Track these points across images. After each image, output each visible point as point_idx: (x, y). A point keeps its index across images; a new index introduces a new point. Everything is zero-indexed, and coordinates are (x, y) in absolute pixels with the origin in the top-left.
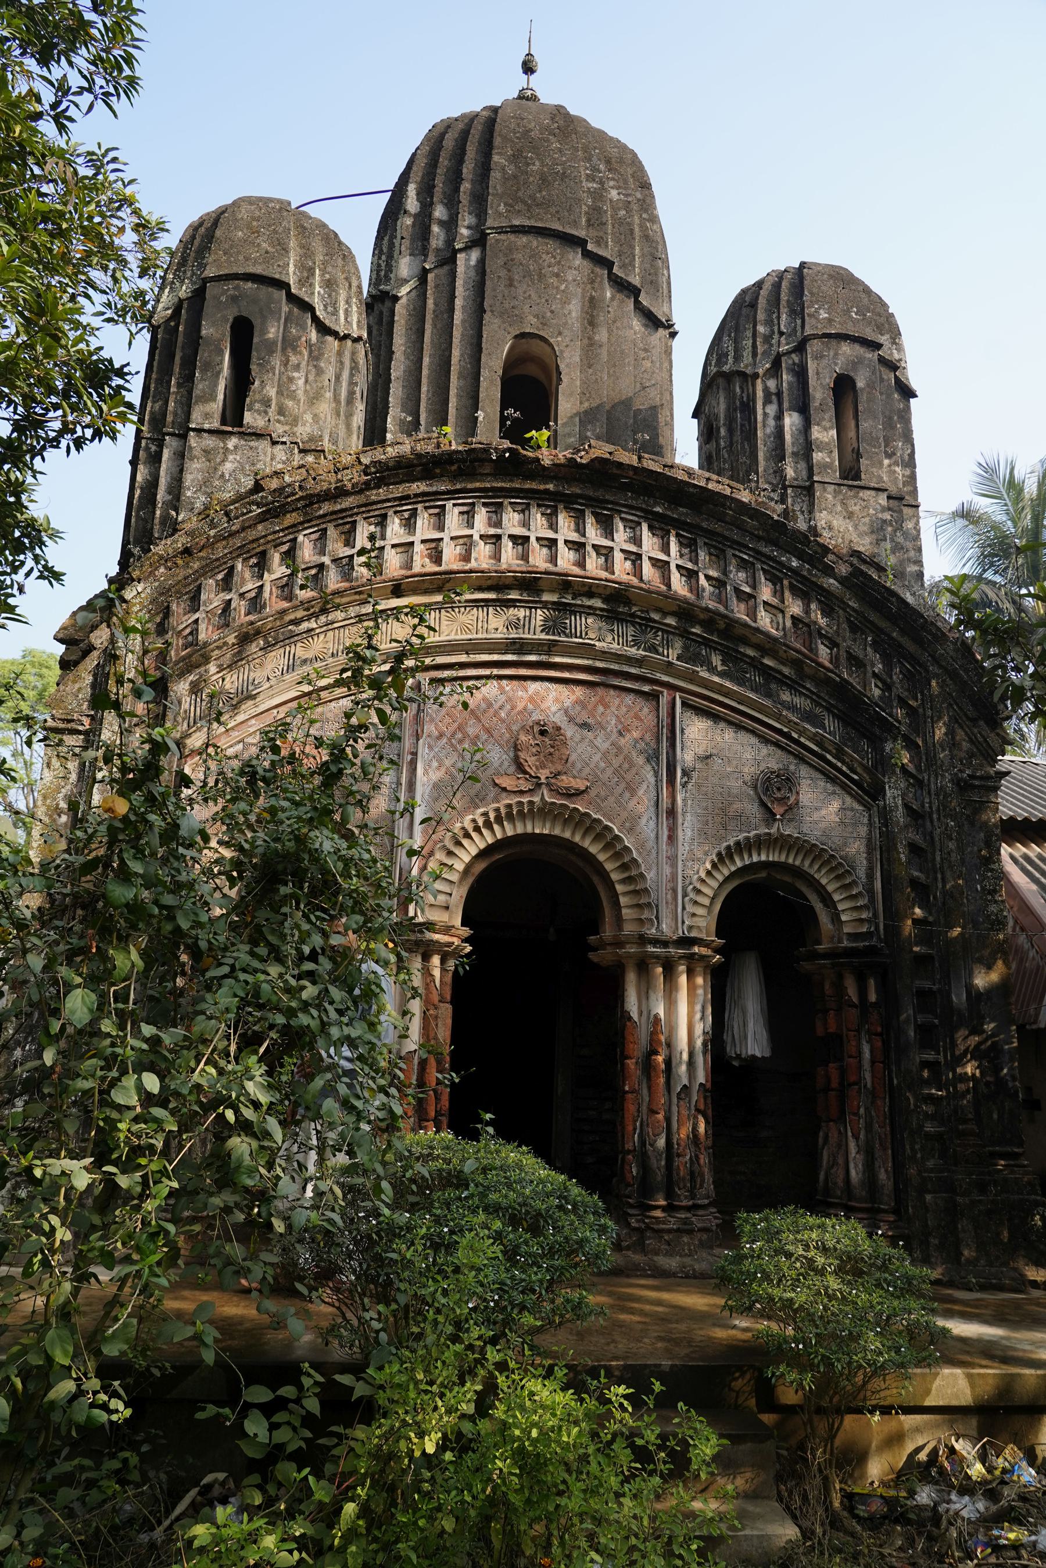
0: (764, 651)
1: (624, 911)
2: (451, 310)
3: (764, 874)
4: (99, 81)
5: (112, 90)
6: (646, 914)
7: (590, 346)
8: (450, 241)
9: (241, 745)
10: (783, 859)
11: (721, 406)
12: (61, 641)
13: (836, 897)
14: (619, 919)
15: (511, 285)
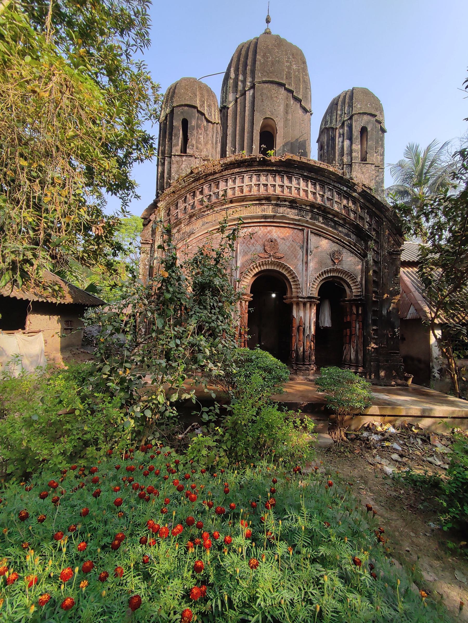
0: (334, 216)
2: (245, 111)
4: (139, 41)
5: (142, 45)
7: (286, 120)
8: (244, 87)
11: (325, 140)
12: (142, 218)
13: (351, 285)
15: (263, 101)
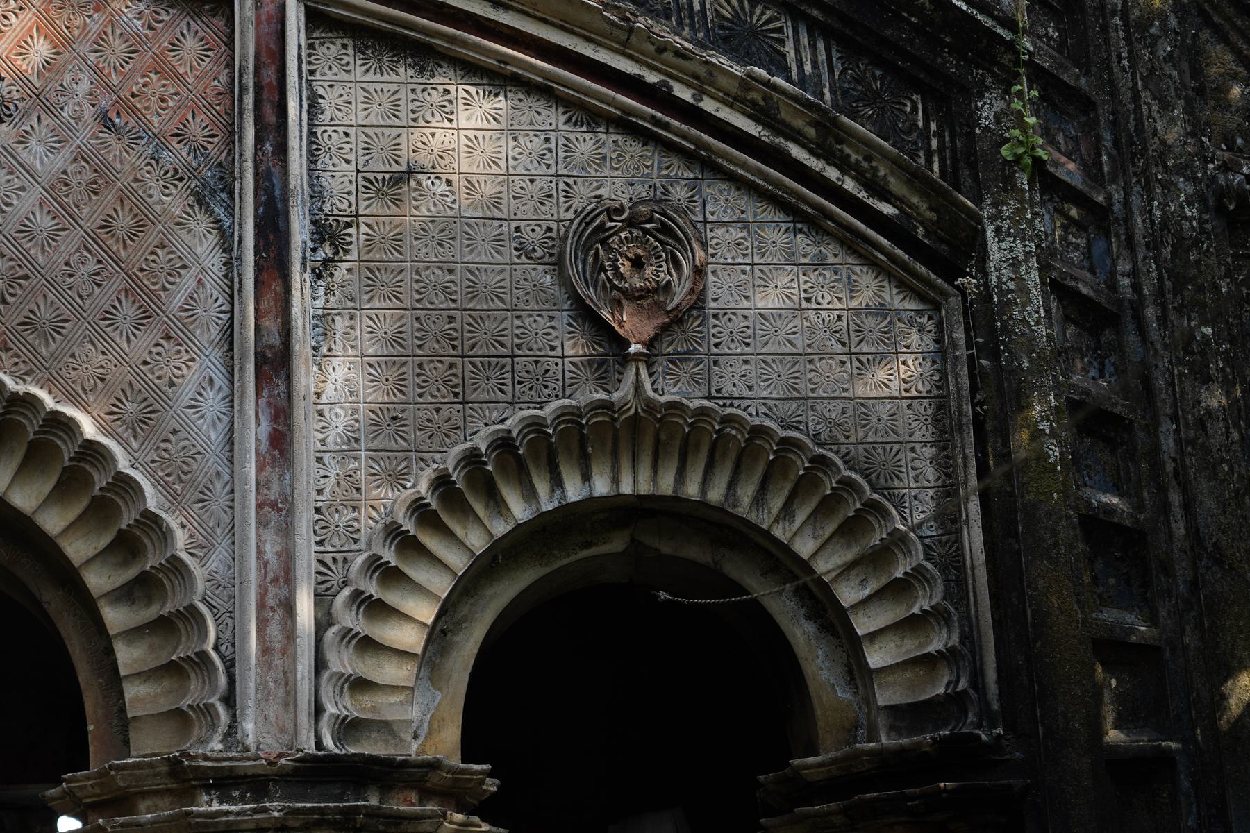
1: (131, 691)
3: (617, 544)
6: (195, 693)
10: (666, 485)
13: (848, 594)
14: (122, 724)
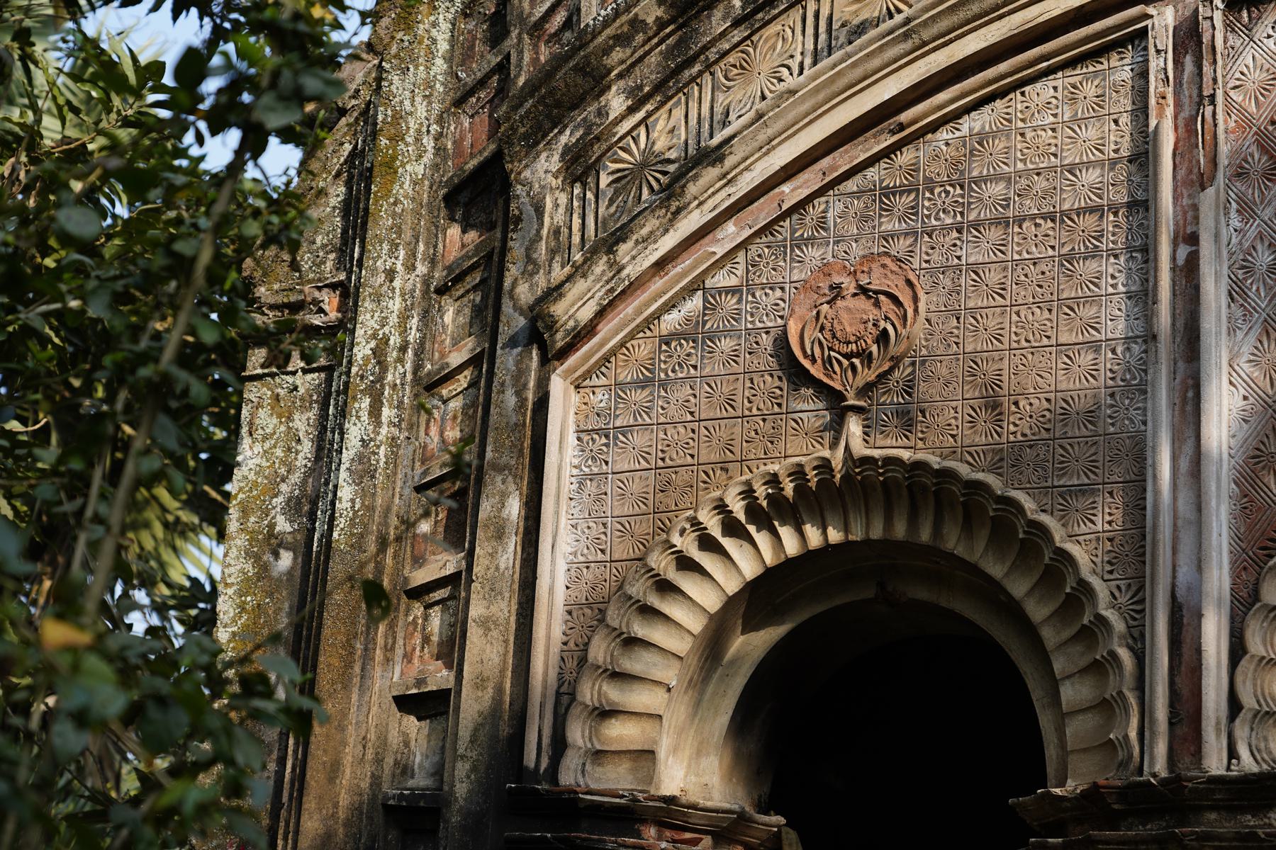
9: (695, 303)
